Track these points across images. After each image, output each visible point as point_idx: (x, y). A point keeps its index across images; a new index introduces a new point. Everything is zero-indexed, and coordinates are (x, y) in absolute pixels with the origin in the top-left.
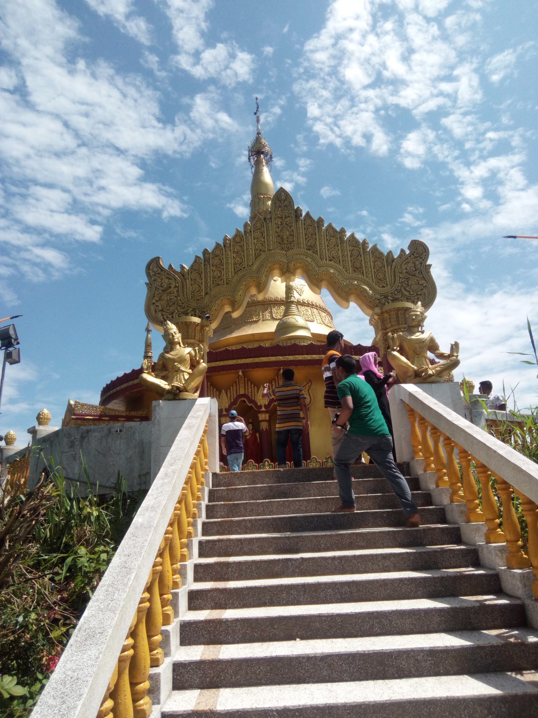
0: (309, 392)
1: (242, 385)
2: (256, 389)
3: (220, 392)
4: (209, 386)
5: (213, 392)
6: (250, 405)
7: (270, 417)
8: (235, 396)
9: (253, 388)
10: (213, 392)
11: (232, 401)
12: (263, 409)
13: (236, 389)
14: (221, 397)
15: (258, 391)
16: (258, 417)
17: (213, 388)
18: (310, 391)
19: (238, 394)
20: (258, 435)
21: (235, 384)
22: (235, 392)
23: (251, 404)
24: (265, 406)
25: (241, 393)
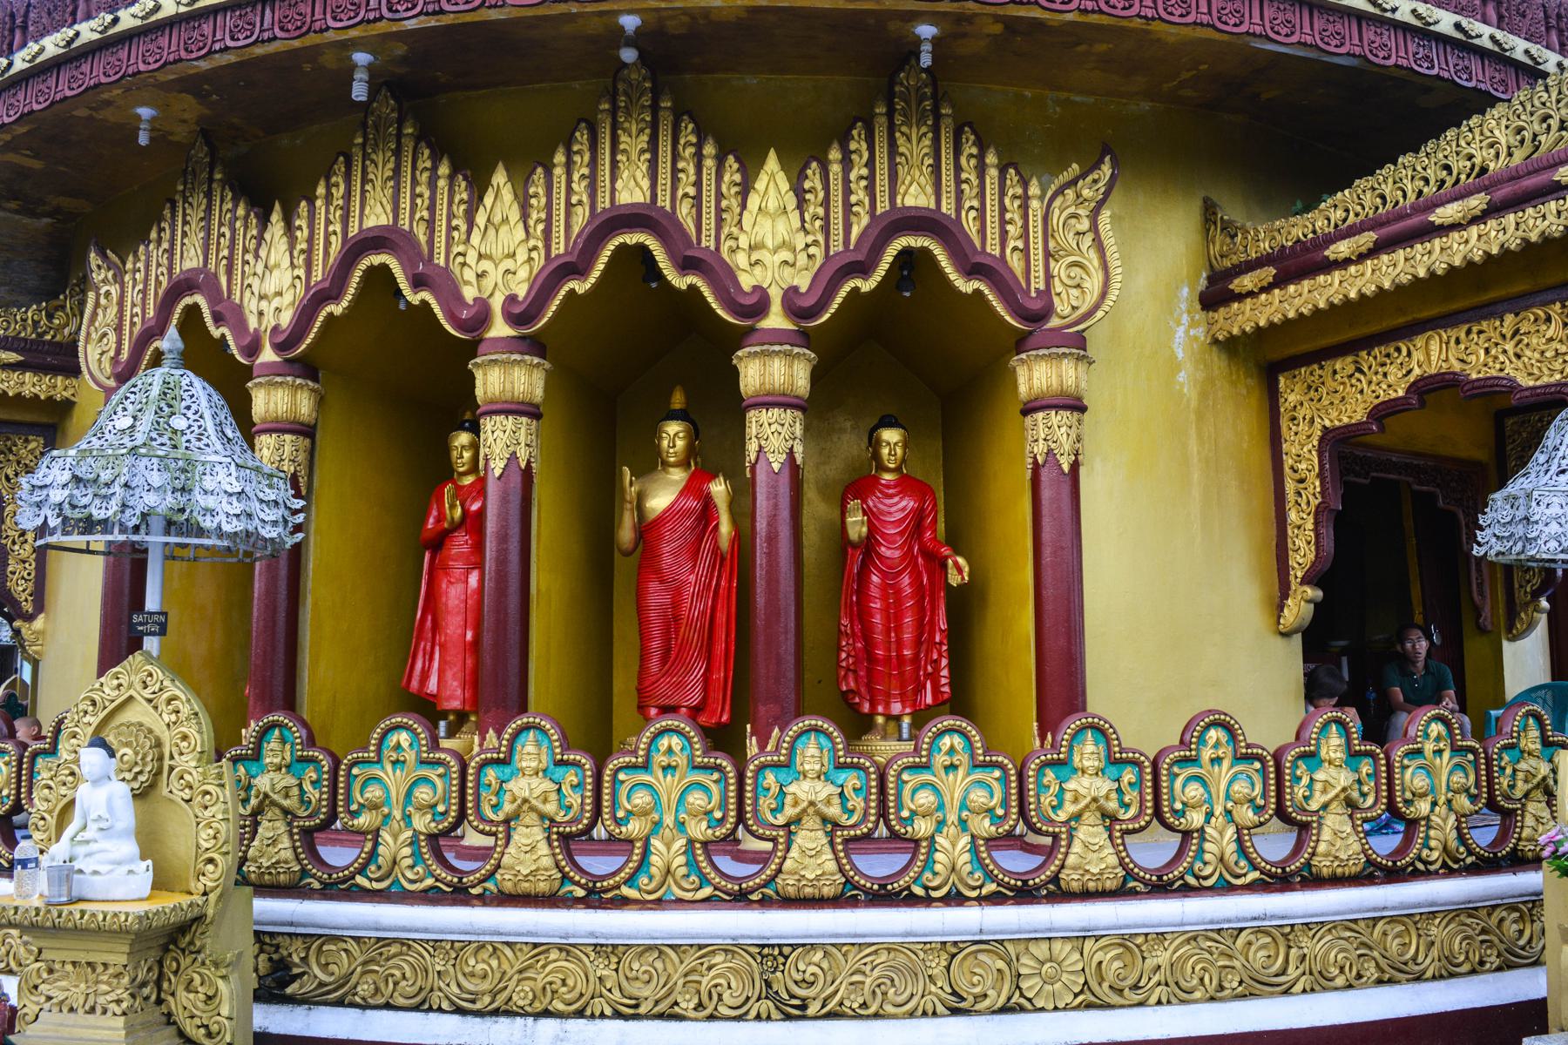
0: (1094, 227)
1: (634, 142)
2: (732, 175)
3: (479, 187)
4: (408, 146)
5: (432, 185)
6: (680, 282)
7: (816, 377)
8: (581, 217)
9: (709, 163)
10: (432, 185)
11: (559, 247)
12: (776, 320)
13: (593, 164)
14: (481, 219)
15: (745, 189)
16: (735, 373)
17: (436, 160)
18: (1105, 216)
19: (604, 202)
20: (719, 489)
21: (582, 136)
22: (580, 187)
23: (692, 279)
24: (791, 293)
25: (624, 198)
